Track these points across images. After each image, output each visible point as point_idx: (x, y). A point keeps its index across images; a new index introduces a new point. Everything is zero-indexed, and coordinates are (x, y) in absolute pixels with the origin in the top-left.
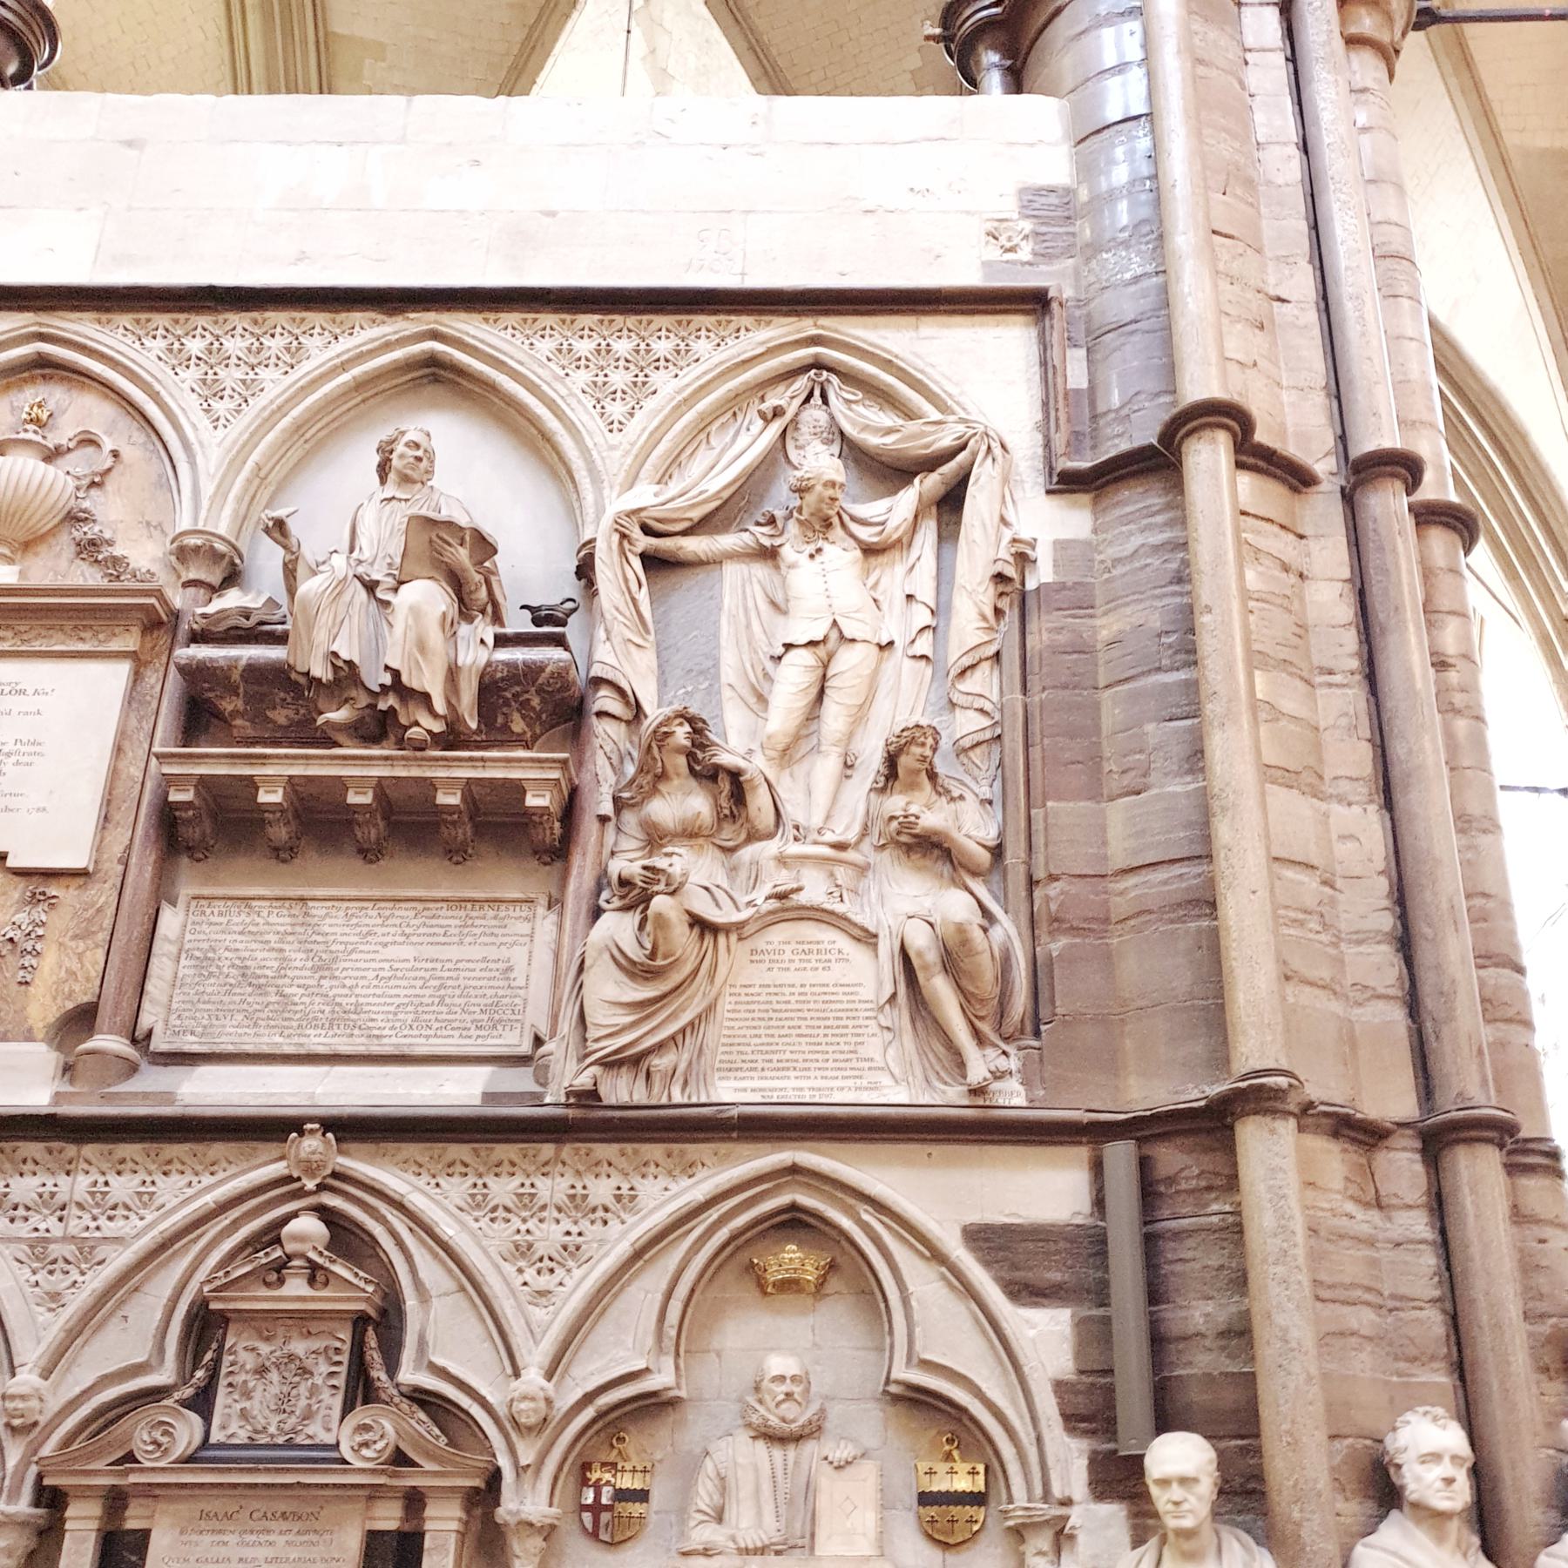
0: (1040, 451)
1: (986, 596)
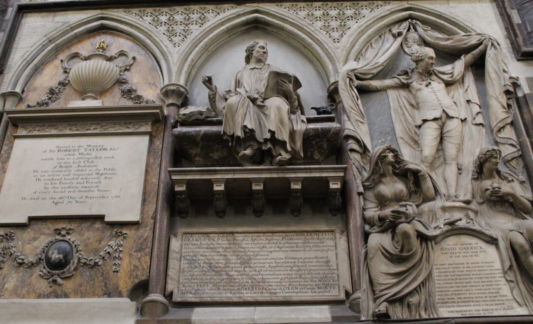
0: (510, 45)
1: (504, 100)
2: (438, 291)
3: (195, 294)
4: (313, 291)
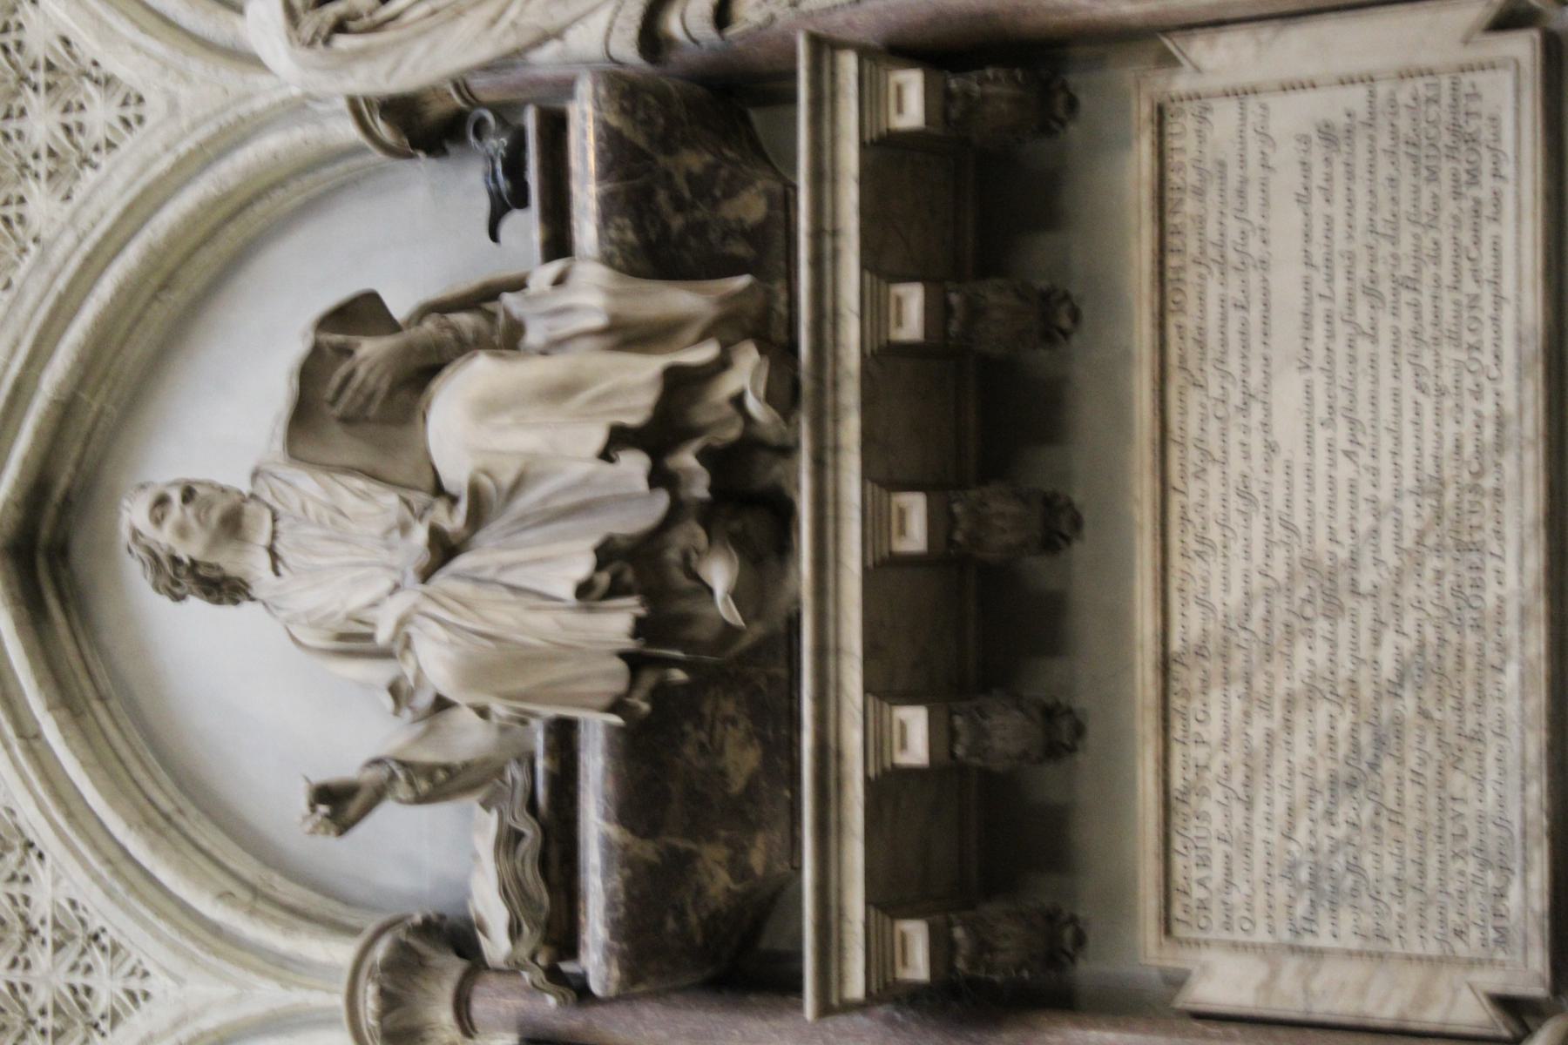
3: (1504, 869)
4: (1487, 210)
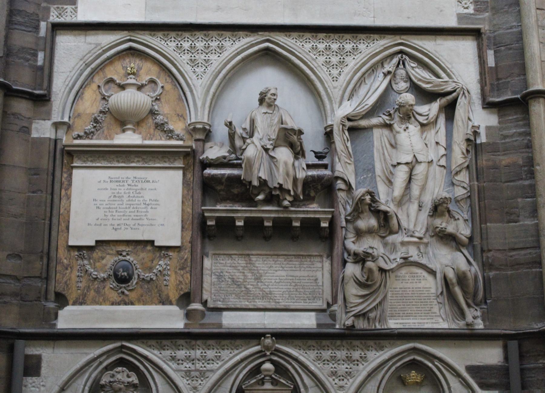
0: (479, 91)
1: (464, 147)
2: (389, 308)
4: (305, 301)
